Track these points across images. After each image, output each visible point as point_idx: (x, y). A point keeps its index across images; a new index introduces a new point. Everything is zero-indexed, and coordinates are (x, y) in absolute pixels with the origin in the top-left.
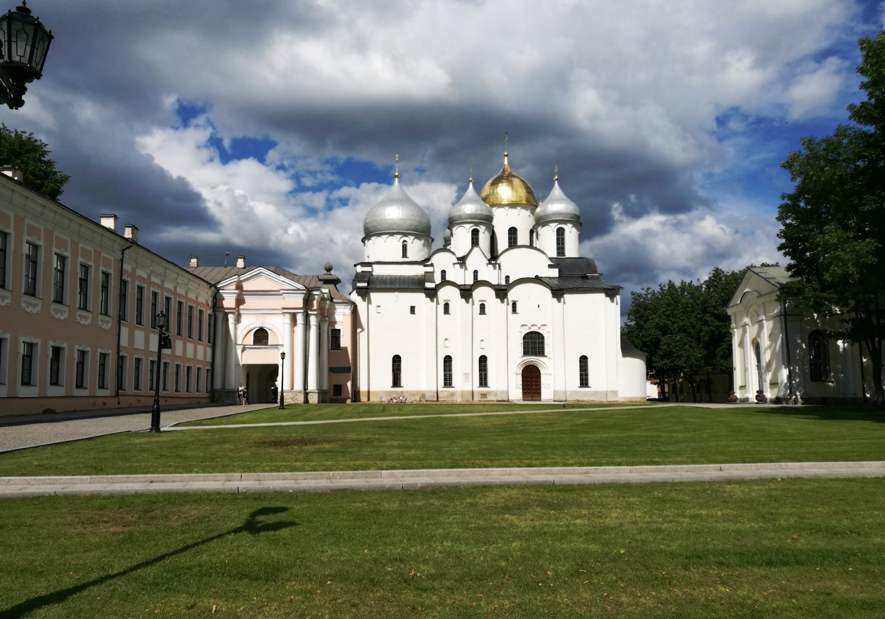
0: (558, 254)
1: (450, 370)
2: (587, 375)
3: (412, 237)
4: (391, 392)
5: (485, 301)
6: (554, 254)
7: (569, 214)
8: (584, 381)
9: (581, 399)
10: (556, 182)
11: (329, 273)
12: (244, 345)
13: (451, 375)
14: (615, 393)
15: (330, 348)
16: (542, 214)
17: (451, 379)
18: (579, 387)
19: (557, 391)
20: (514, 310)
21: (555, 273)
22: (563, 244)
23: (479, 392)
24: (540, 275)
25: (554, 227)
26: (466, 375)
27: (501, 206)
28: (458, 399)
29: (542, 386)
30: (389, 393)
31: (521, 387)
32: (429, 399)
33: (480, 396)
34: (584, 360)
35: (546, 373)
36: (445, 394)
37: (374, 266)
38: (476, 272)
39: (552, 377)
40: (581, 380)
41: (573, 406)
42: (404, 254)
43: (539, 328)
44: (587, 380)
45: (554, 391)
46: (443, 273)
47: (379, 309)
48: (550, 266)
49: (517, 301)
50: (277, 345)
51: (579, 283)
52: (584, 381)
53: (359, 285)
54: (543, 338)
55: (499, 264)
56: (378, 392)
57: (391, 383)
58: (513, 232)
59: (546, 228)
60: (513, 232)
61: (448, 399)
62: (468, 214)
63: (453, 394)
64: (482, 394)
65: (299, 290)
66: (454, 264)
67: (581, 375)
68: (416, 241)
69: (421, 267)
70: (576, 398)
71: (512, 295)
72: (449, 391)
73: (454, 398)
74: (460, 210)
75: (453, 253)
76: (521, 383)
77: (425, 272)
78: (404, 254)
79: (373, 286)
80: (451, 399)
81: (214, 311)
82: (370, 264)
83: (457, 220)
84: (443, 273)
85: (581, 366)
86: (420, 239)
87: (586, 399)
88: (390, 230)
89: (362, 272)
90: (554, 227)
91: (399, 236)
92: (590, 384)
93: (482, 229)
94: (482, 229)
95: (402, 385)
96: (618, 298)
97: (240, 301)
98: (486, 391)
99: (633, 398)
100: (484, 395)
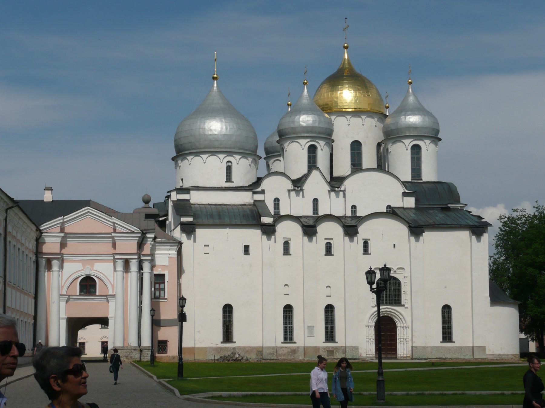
0: (413, 178)
1: (291, 322)
2: (450, 328)
3: (238, 157)
4: (221, 348)
5: (332, 239)
6: (408, 177)
7: (426, 128)
8: (447, 335)
9: (444, 357)
11: (147, 205)
12: (69, 296)
13: (291, 329)
14: (483, 349)
15: (153, 297)
16: (393, 127)
17: (291, 333)
18: (441, 342)
19: (416, 347)
20: (366, 250)
21: (410, 202)
23: (325, 348)
24: (392, 206)
25: (409, 143)
26: (311, 328)
27: (342, 113)
28: (300, 357)
29: (398, 342)
30: (218, 350)
31: (374, 342)
32: (267, 357)
33: (326, 353)
34: (447, 310)
35: (402, 325)
36: (286, 351)
37: (192, 192)
38: (316, 201)
39: (409, 330)
40: (444, 333)
41: (433, 364)
42: (229, 178)
43: (395, 272)
44: (450, 333)
45: (412, 347)
46: (277, 201)
47: (207, 249)
48: (405, 194)
49: (369, 240)
50: (106, 296)
51: (440, 217)
52: (447, 335)
53: (184, 219)
54: (399, 283)
55: (343, 191)
56: (206, 348)
57: (221, 338)
58: (356, 146)
59: (399, 145)
60: (356, 146)
62: (304, 127)
63: (294, 351)
64: (328, 351)
65: (133, 232)
66: (289, 191)
67: (444, 328)
68: (243, 160)
69: (250, 194)
70: (438, 355)
71: (364, 230)
72: (289, 347)
73: (296, 355)
74: (293, 122)
75: (288, 177)
76: (374, 338)
77: (255, 201)
78: (229, 178)
79: (200, 221)
80: (292, 357)
81: (37, 257)
82: (187, 191)
83: (290, 134)
84: (277, 201)
85: (443, 318)
86: (246, 158)
87: (449, 356)
88: (210, 148)
89: (178, 200)
90: (409, 143)
91: (222, 156)
92: (454, 338)
93: (321, 145)
94: (321, 145)
95: (234, 340)
96: (485, 237)
97: (63, 245)
98: (332, 347)
99: (503, 355)
100: (331, 352)
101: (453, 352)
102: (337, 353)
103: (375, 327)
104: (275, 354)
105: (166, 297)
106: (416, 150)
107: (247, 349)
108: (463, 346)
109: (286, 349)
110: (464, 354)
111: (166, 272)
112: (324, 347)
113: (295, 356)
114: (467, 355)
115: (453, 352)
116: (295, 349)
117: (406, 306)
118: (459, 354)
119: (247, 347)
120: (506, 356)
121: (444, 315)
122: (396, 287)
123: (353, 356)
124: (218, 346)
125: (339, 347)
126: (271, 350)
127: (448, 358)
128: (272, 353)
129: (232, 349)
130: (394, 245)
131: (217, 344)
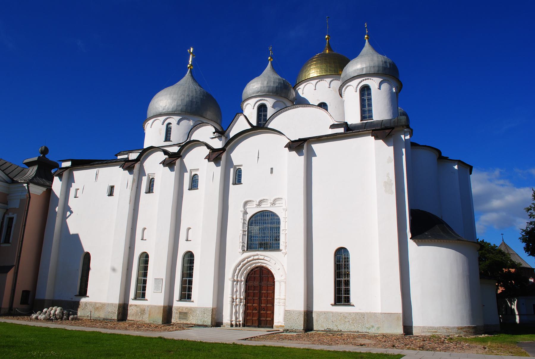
0: (363, 118)
9: (335, 329)
10: (367, 40)
18: (332, 305)
22: (370, 105)
33: (177, 315)
49: (241, 166)
61: (138, 319)
63: (143, 311)
64: (180, 313)
72: (139, 305)
78: (167, 138)
80: (141, 319)
91: (162, 118)
98: (186, 308)
100: (184, 314)
101: (351, 321)
102: (191, 316)
103: (247, 281)
104: (117, 313)
105: (11, 241)
106: (365, 91)
107: (97, 306)
108: (367, 313)
109: (135, 307)
110: (367, 327)
111: (15, 216)
112: (178, 307)
113: (143, 318)
114: (373, 327)
115: (351, 321)
116: (144, 307)
117: (284, 251)
118: (360, 325)
119: (98, 303)
120: (445, 331)
121: (346, 263)
122: (275, 226)
123: (204, 321)
124: (73, 300)
125: (194, 308)
126: (113, 308)
127: (343, 330)
128: (113, 311)
129: (84, 304)
130: (272, 169)
131: (72, 299)
